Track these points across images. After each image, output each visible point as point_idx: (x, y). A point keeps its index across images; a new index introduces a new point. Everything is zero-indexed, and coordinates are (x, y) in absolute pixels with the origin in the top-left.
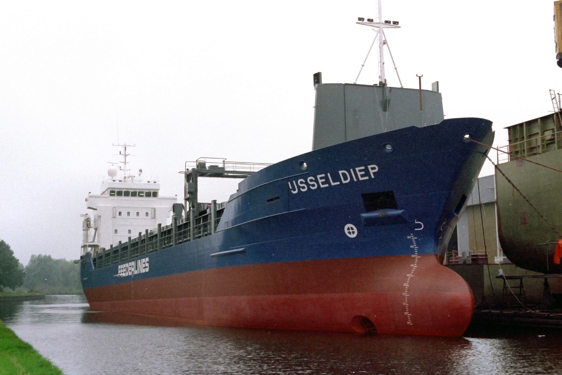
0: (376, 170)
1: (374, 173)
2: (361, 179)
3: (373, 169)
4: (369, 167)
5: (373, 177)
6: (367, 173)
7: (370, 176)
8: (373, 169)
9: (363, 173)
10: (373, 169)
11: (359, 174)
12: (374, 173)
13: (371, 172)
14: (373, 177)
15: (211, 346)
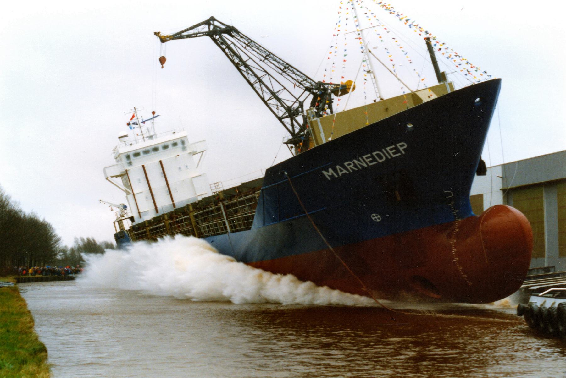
0: (406, 146)
1: (404, 150)
2: (394, 156)
3: (402, 146)
4: (398, 145)
5: (403, 152)
6: (398, 151)
7: (401, 153)
8: (401, 146)
9: (394, 151)
10: (402, 146)
11: (391, 152)
12: (404, 150)
13: (401, 149)
14: (403, 152)
15: (88, 349)
